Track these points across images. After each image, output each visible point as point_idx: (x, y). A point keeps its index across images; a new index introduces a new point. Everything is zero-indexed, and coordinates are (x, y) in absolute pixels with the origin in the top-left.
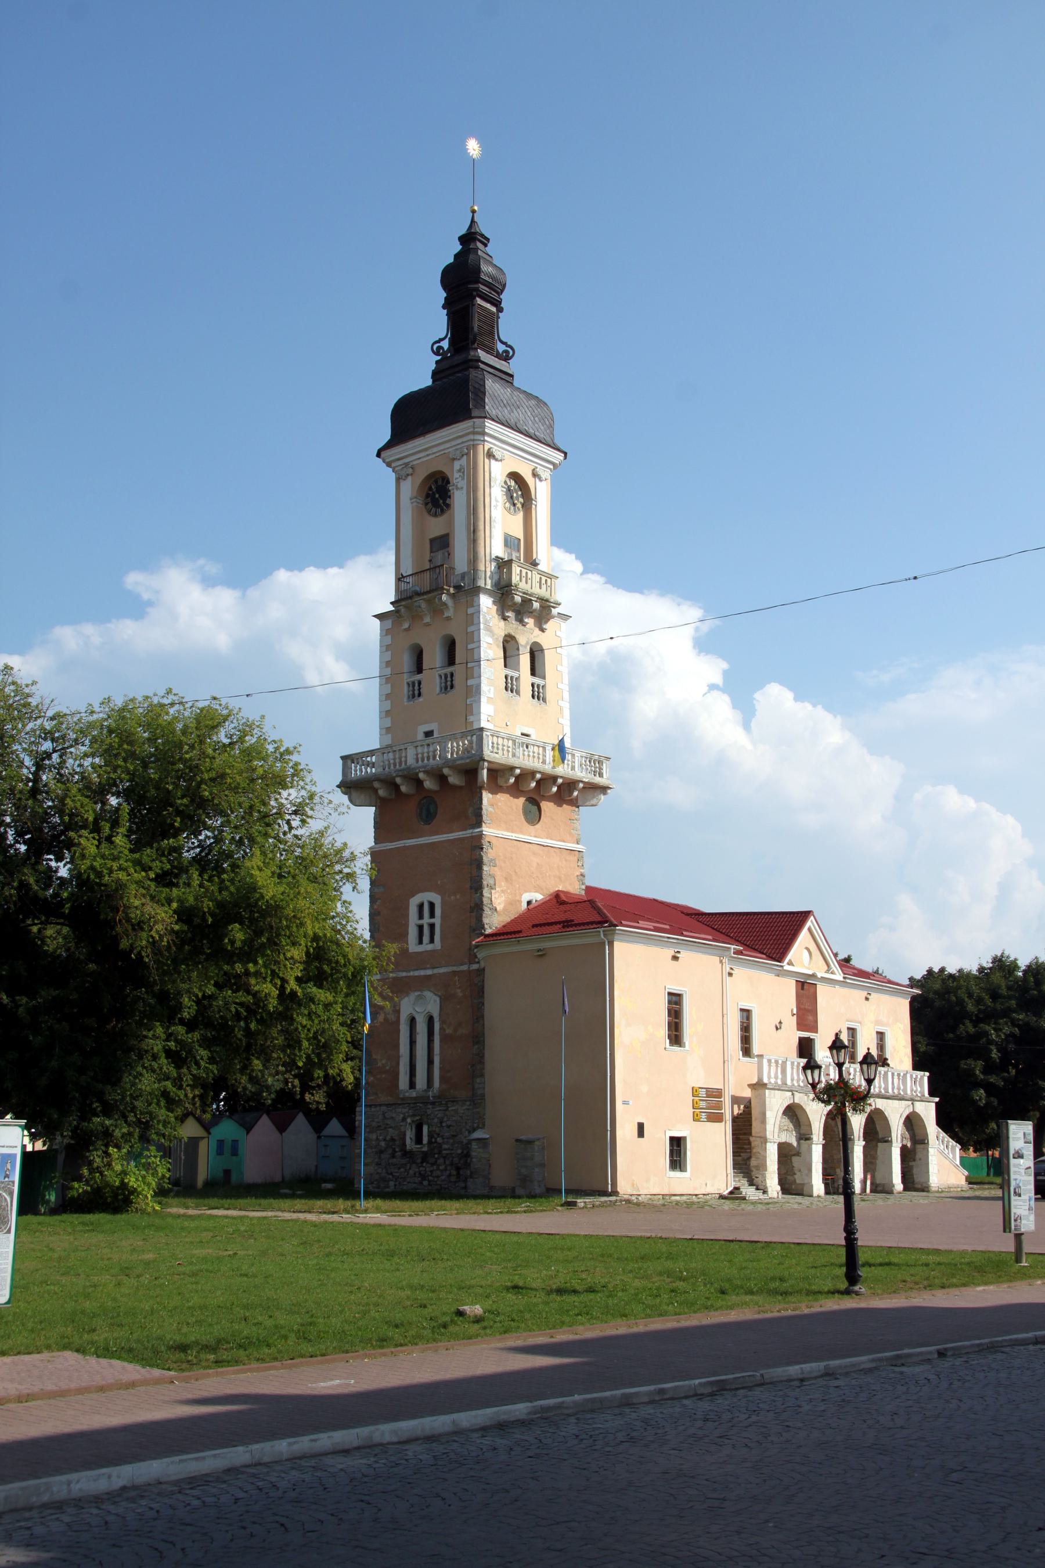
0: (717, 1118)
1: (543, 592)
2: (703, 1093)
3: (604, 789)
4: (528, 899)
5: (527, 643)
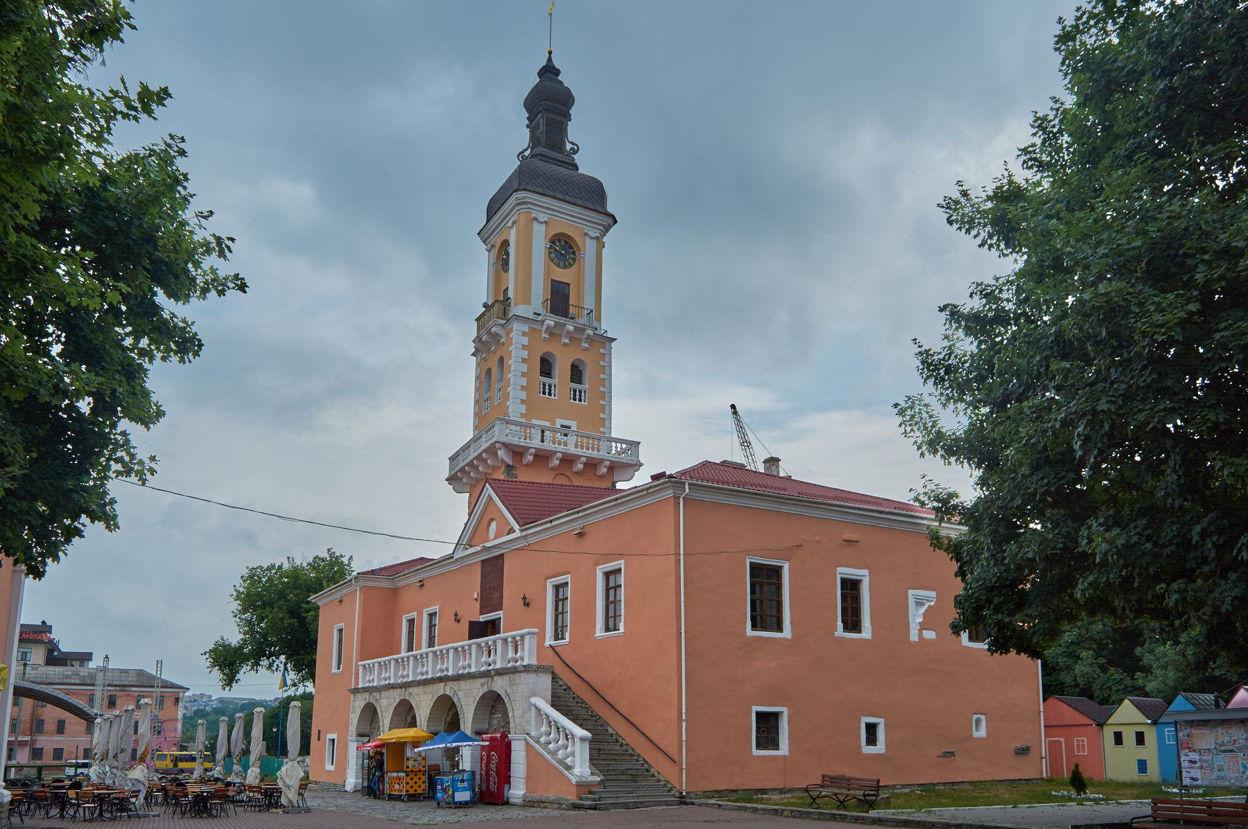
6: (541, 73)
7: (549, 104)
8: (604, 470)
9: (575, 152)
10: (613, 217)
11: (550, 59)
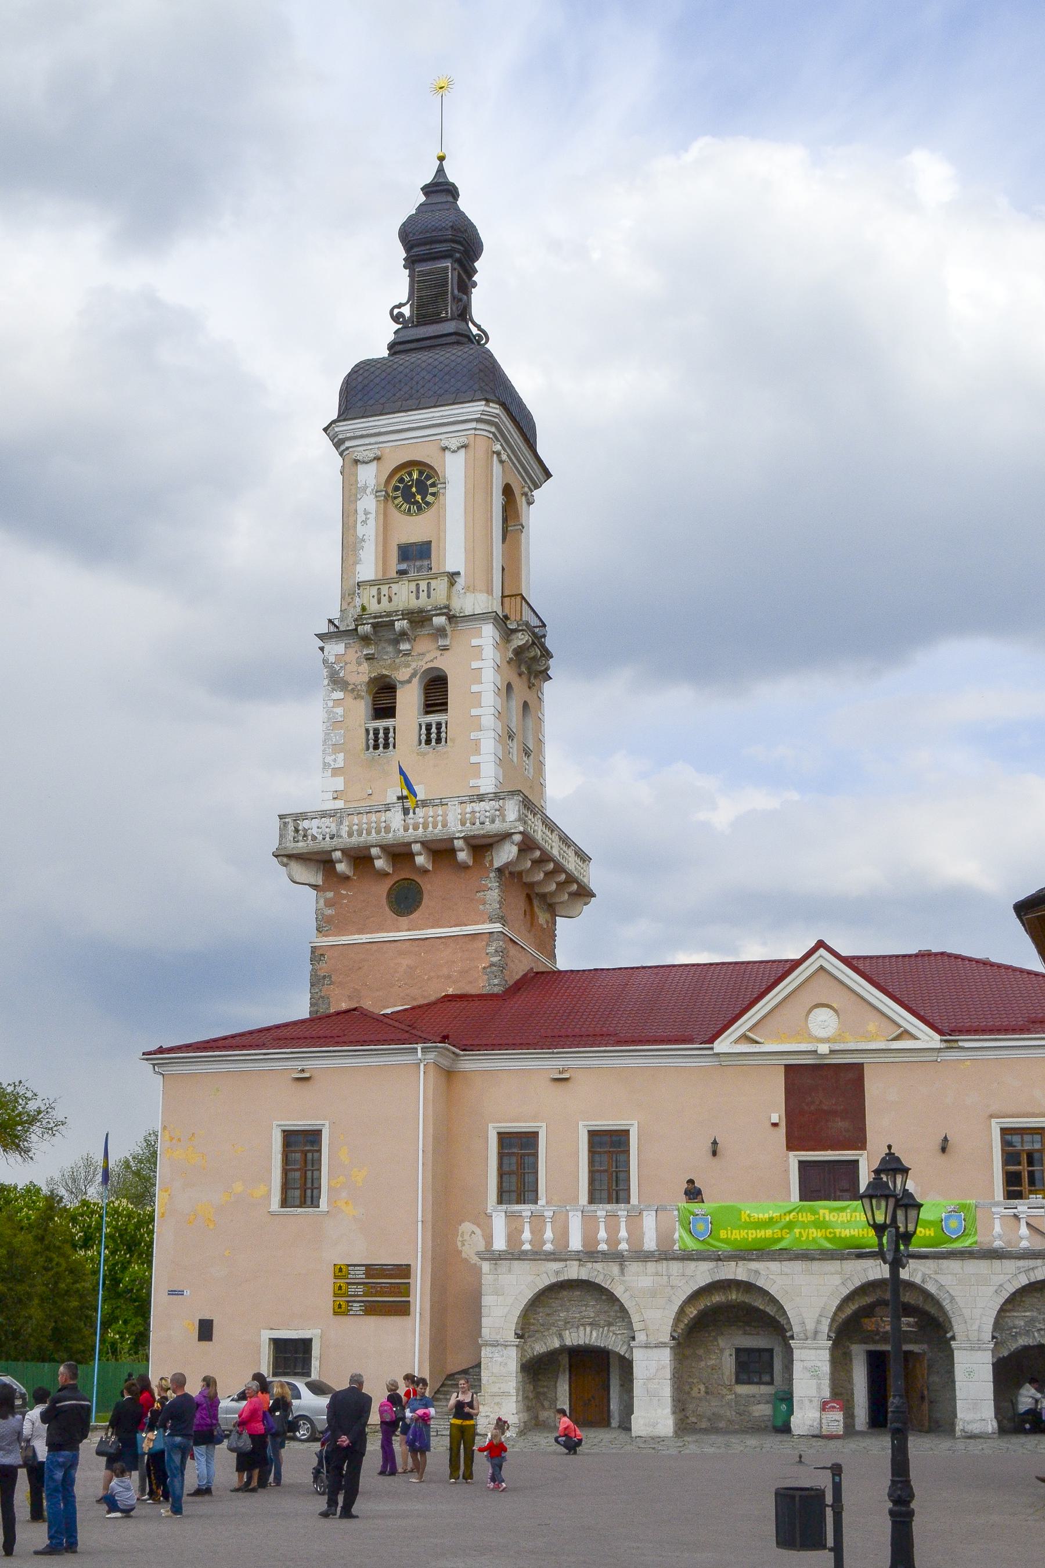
0: (402, 1309)
1: (423, 602)
2: (360, 1273)
3: (506, 836)
5: (413, 675)
11: (441, 171)
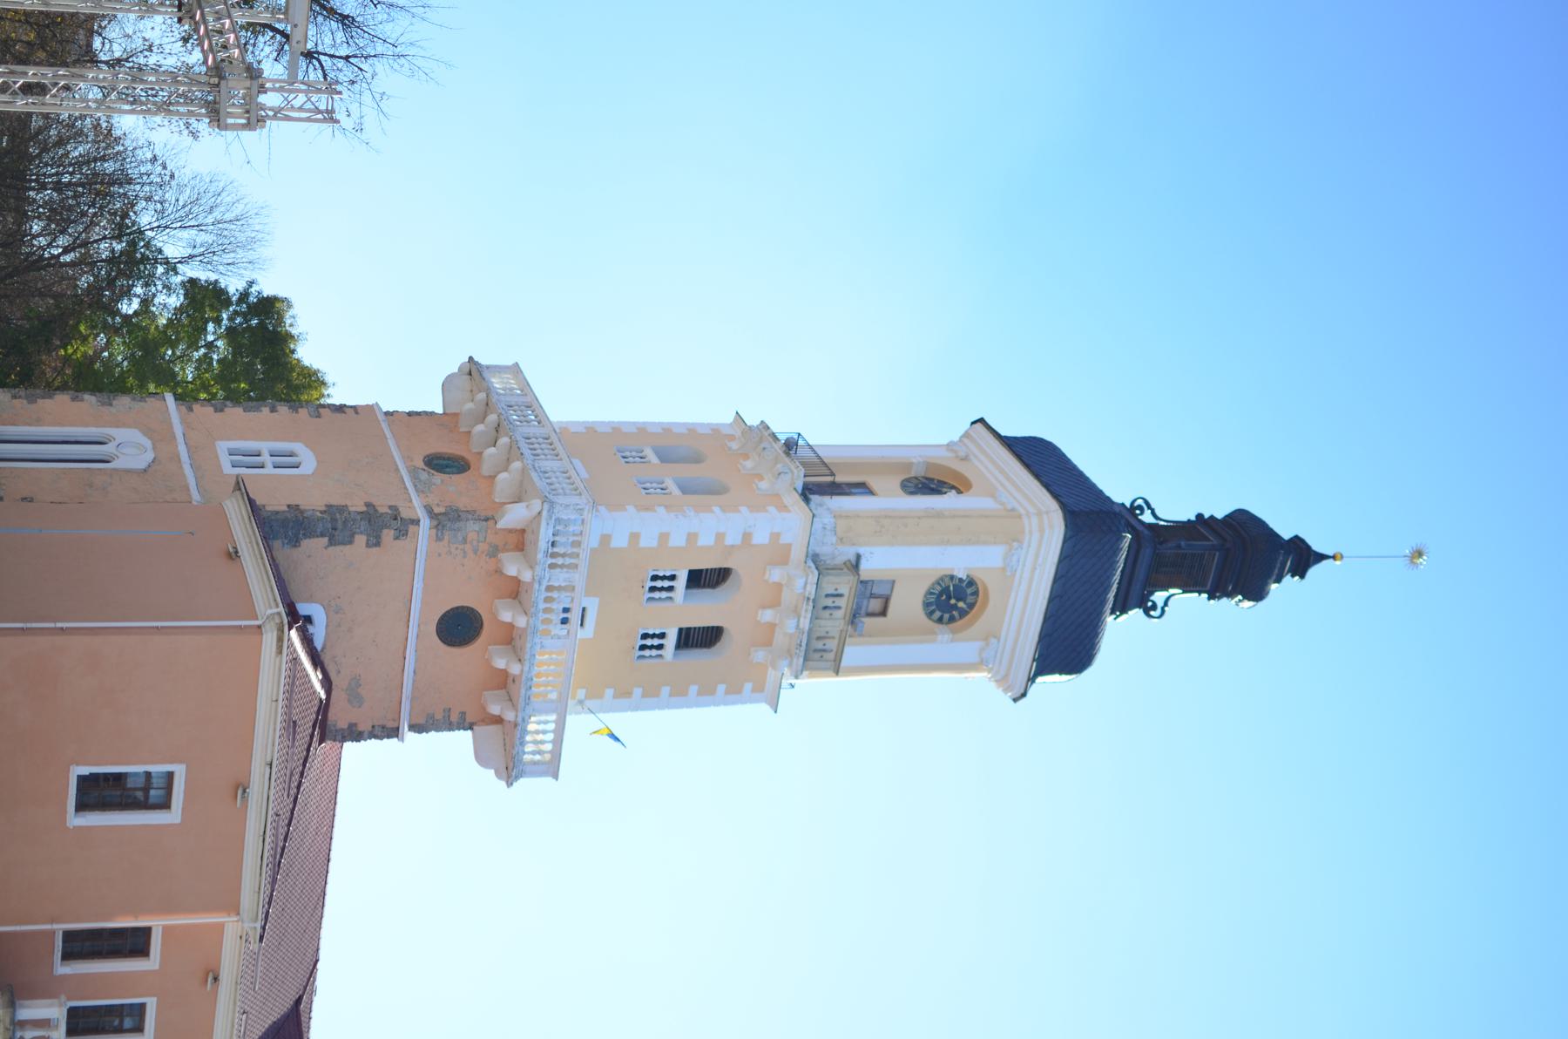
4: (316, 619)
6: (1297, 542)
7: (1239, 556)
8: (495, 709)
9: (1147, 612)
10: (1024, 695)
11: (1322, 557)
